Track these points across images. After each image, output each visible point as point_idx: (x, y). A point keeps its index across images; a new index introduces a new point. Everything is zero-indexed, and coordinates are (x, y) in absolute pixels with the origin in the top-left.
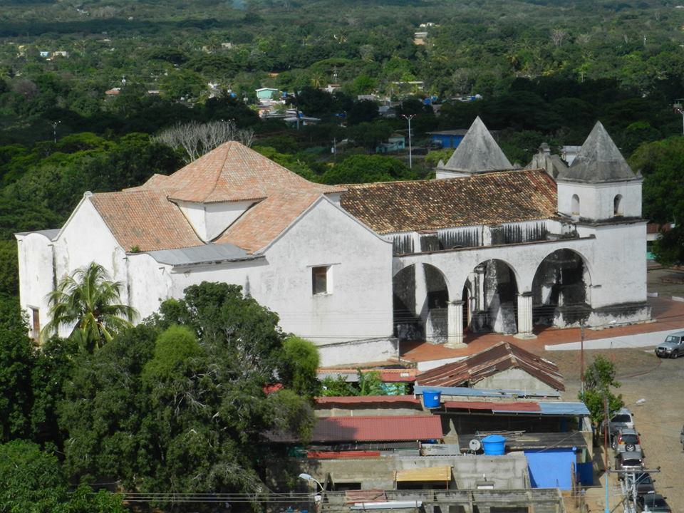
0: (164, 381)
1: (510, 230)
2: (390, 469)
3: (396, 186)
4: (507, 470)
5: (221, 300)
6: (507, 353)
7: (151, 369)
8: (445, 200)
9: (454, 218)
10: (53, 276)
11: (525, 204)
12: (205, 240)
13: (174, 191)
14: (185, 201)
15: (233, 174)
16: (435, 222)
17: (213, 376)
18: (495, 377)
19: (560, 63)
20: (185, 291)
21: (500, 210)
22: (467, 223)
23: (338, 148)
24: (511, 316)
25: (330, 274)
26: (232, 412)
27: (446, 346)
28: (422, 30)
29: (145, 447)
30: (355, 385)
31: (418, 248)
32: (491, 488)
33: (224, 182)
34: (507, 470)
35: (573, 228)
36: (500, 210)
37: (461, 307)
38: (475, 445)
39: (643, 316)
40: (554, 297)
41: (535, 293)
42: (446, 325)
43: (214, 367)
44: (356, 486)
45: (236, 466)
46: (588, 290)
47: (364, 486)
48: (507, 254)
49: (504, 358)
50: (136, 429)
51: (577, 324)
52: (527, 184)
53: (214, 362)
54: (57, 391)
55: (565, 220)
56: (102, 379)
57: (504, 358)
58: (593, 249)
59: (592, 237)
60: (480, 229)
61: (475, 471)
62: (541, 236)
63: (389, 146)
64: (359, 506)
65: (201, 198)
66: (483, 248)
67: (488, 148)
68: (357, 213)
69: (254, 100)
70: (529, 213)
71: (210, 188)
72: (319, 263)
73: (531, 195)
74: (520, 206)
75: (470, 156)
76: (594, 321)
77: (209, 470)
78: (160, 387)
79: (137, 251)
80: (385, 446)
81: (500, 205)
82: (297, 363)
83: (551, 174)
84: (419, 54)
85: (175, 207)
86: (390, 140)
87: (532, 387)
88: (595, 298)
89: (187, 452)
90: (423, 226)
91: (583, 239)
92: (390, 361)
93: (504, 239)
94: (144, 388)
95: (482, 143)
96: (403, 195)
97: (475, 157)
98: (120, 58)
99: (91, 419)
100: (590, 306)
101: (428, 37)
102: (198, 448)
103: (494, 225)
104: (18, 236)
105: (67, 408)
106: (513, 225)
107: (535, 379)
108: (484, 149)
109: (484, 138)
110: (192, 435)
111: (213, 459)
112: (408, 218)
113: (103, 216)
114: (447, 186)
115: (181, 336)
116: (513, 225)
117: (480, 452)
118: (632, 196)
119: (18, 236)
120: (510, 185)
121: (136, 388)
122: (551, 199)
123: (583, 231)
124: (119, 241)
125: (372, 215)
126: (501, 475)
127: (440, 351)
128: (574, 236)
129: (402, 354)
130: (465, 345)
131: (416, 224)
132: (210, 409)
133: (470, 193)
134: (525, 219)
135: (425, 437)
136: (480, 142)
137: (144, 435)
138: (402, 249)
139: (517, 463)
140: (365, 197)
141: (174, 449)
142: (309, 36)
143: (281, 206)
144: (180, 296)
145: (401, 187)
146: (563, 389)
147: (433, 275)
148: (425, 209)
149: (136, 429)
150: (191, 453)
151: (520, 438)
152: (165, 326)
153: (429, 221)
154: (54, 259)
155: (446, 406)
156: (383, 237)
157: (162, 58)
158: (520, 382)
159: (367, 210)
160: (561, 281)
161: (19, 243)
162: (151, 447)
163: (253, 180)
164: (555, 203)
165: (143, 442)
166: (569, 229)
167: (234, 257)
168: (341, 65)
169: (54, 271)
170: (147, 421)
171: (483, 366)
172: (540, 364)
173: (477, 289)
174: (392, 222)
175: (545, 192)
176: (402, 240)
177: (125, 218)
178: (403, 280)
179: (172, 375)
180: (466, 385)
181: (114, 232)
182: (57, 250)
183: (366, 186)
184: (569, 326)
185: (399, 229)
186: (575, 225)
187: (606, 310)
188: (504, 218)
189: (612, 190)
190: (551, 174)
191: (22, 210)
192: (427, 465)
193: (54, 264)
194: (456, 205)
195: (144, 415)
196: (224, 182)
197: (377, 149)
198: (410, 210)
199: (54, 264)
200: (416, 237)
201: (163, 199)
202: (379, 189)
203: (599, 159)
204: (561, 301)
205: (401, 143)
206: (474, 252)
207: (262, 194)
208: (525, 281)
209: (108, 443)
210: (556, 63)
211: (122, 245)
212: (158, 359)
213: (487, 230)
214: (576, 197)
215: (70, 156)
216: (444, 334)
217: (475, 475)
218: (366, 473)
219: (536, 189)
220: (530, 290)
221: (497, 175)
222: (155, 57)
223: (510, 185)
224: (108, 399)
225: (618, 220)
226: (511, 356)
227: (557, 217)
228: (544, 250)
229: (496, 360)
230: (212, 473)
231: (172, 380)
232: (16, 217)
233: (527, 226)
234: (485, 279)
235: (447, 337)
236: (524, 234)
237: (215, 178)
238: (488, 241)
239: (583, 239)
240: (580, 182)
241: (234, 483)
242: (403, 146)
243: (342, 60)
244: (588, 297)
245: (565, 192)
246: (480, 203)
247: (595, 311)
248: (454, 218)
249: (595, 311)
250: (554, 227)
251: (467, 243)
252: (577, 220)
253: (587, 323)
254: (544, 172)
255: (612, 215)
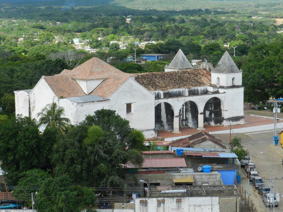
0: (91, 146)
1: (194, 90)
2: (171, 178)
3: (153, 74)
4: (214, 178)
5: (109, 115)
6: (203, 135)
7: (87, 141)
8: (171, 79)
9: (175, 86)
10: (29, 106)
11: (199, 81)
12: (85, 93)
13: (74, 76)
14: (79, 79)
15: (96, 70)
16: (168, 87)
17: (109, 144)
18: (201, 144)
19: (181, 30)
20: (95, 112)
21: (191, 83)
22: (179, 87)
23: (109, 60)
24: (195, 122)
25: (133, 106)
26: (116, 157)
27: (173, 132)
28: (129, 18)
29: (85, 170)
30: (148, 147)
31: (162, 96)
32: (207, 185)
33: (93, 72)
34: (214, 178)
35: (217, 89)
36: (191, 83)
37: (178, 118)
38: (200, 169)
39: (242, 122)
40: (210, 115)
41: (204, 113)
42: (173, 125)
43: (109, 141)
44: (158, 184)
45: (117, 177)
46: (223, 112)
47: (161, 184)
48: (193, 99)
49: (203, 137)
50: (82, 163)
51: (218, 124)
52: (200, 74)
53: (108, 139)
54: (50, 150)
55: (214, 86)
56: (68, 145)
57: (203, 137)
58: (225, 97)
59: (225, 93)
60: (184, 89)
61: (202, 179)
62: (206, 92)
63: (127, 59)
64: (163, 192)
65: (85, 78)
66: (185, 96)
67: (184, 60)
68: (140, 83)
69: (73, 42)
70: (201, 84)
71: (88, 74)
72: (129, 102)
73: (201, 78)
74: (198, 81)
75: (177, 63)
76: (225, 123)
77: (108, 179)
78: (90, 148)
79: (62, 97)
80: (166, 169)
81: (190, 81)
82: (138, 139)
83: (208, 70)
84: (129, 27)
85: (75, 82)
86: (128, 57)
87: (215, 148)
88: (226, 115)
89: (100, 172)
90: (164, 89)
91: (220, 93)
92: (154, 138)
93: (193, 93)
94: (84, 148)
95: (182, 58)
96: (156, 77)
97: (179, 64)
98: (21, 27)
99: (63, 160)
100: (223, 118)
101: (131, 20)
102: (105, 171)
103: (189, 88)
104: (15, 92)
105: (55, 157)
106: (196, 88)
107: (216, 145)
108: (183, 61)
109: (182, 56)
110: (102, 166)
111: (110, 175)
112: (158, 86)
113: (49, 85)
114: (171, 74)
115: (97, 129)
116: (196, 88)
117: (202, 171)
118: (238, 77)
119: (15, 92)
120: (194, 74)
121: (81, 148)
122: (208, 79)
123: (221, 91)
124: (55, 94)
125: (145, 85)
126: (211, 180)
127: (171, 134)
128: (217, 92)
129: (158, 135)
130: (180, 132)
131: (161, 88)
132: (109, 156)
133: (180, 77)
134: (200, 86)
135: (180, 166)
136: (181, 58)
137: (85, 166)
138: (158, 97)
139: (217, 176)
140: (142, 78)
141: (95, 171)
142: (88, 20)
143: (115, 81)
144: (92, 114)
145: (155, 74)
146: (226, 148)
147: (168, 106)
148: (164, 83)
149: (82, 163)
150: (102, 172)
151: (216, 167)
152: (90, 124)
153: (166, 87)
154: (29, 100)
155: (186, 154)
156: (151, 92)
157: (36, 27)
158: (210, 145)
159: (143, 82)
160: (213, 109)
161: (15, 95)
162: (87, 170)
163: (103, 71)
164: (210, 80)
165: (84, 168)
166: (215, 90)
167: (99, 100)
168: (102, 30)
169: (29, 105)
170: (86, 160)
171: (196, 140)
172: (215, 139)
173: (183, 112)
174: (153, 87)
175: (206, 76)
176: (157, 93)
177: (57, 85)
178: (158, 108)
179: (94, 144)
180: (189, 147)
181: (53, 91)
182: (31, 97)
183: (142, 74)
184: (216, 125)
185: (156, 89)
186: (218, 88)
187: (229, 119)
188: (193, 86)
189: (231, 76)
190: (208, 70)
191: (13, 82)
192: (184, 176)
193: (29, 102)
194: (175, 81)
195: (84, 158)
196: (93, 72)
197: (123, 60)
198: (159, 83)
199: (29, 102)
200: (161, 93)
201: (70, 79)
202: (147, 75)
203: (227, 65)
204: (213, 116)
205: (131, 59)
206: (183, 98)
207: (107, 77)
208: (201, 109)
209: (71, 168)
210: (180, 30)
211: (57, 95)
212: (89, 138)
213: (187, 90)
214: (218, 78)
215: (16, 62)
216: (172, 128)
217: (202, 180)
218: (161, 179)
219: (203, 75)
220: (203, 112)
221: (189, 70)
222: (33, 27)
223: (194, 74)
224: (71, 152)
225: (233, 87)
226: (206, 136)
227: (211, 85)
228: (207, 97)
229: (199, 137)
230: (110, 180)
231: (94, 145)
232: (11, 85)
233: (200, 88)
234: (186, 108)
235: (173, 129)
236: (200, 92)
237: (89, 71)
238: (187, 94)
239: (220, 93)
240: (220, 73)
241: (118, 183)
242: (132, 60)
243: (102, 29)
244: (223, 114)
245: (214, 77)
246: (183, 80)
247: (225, 120)
248: (175, 86)
249: (225, 120)
250: (211, 89)
251: (179, 95)
252: (219, 87)
253: (222, 124)
254: (205, 69)
255: (232, 85)
